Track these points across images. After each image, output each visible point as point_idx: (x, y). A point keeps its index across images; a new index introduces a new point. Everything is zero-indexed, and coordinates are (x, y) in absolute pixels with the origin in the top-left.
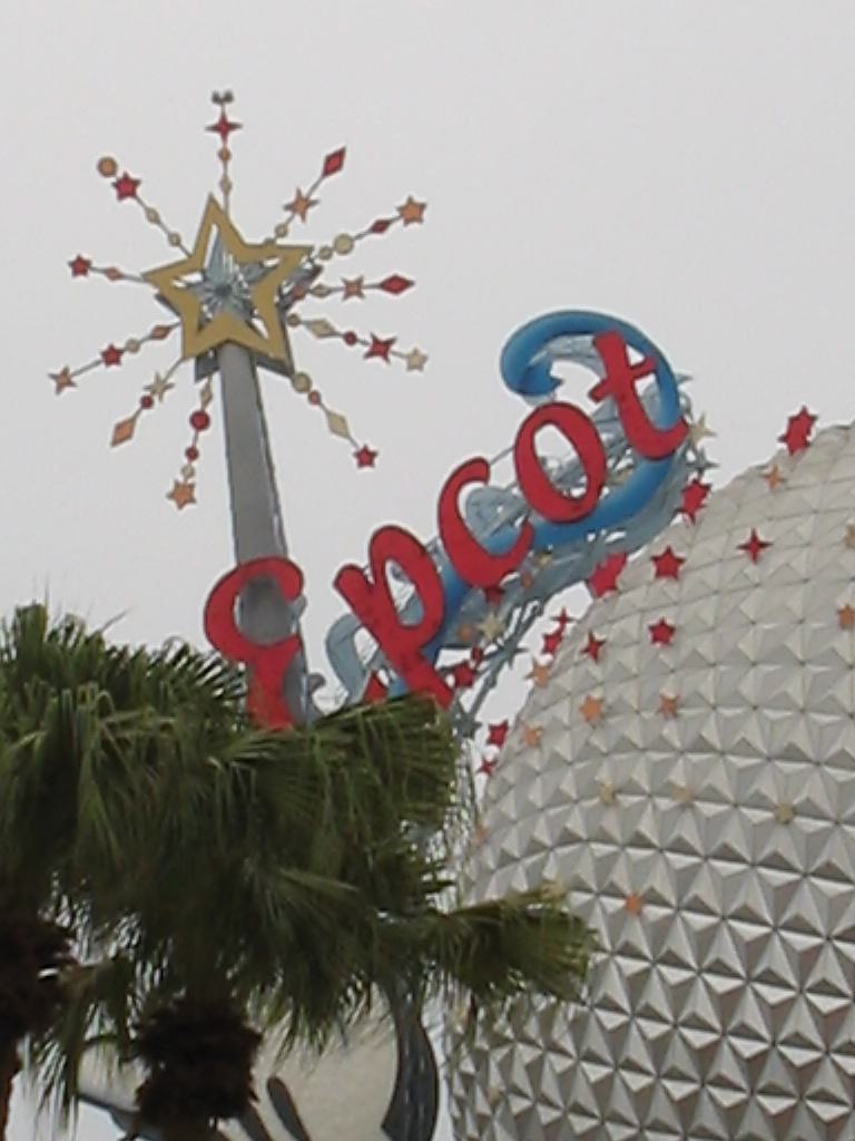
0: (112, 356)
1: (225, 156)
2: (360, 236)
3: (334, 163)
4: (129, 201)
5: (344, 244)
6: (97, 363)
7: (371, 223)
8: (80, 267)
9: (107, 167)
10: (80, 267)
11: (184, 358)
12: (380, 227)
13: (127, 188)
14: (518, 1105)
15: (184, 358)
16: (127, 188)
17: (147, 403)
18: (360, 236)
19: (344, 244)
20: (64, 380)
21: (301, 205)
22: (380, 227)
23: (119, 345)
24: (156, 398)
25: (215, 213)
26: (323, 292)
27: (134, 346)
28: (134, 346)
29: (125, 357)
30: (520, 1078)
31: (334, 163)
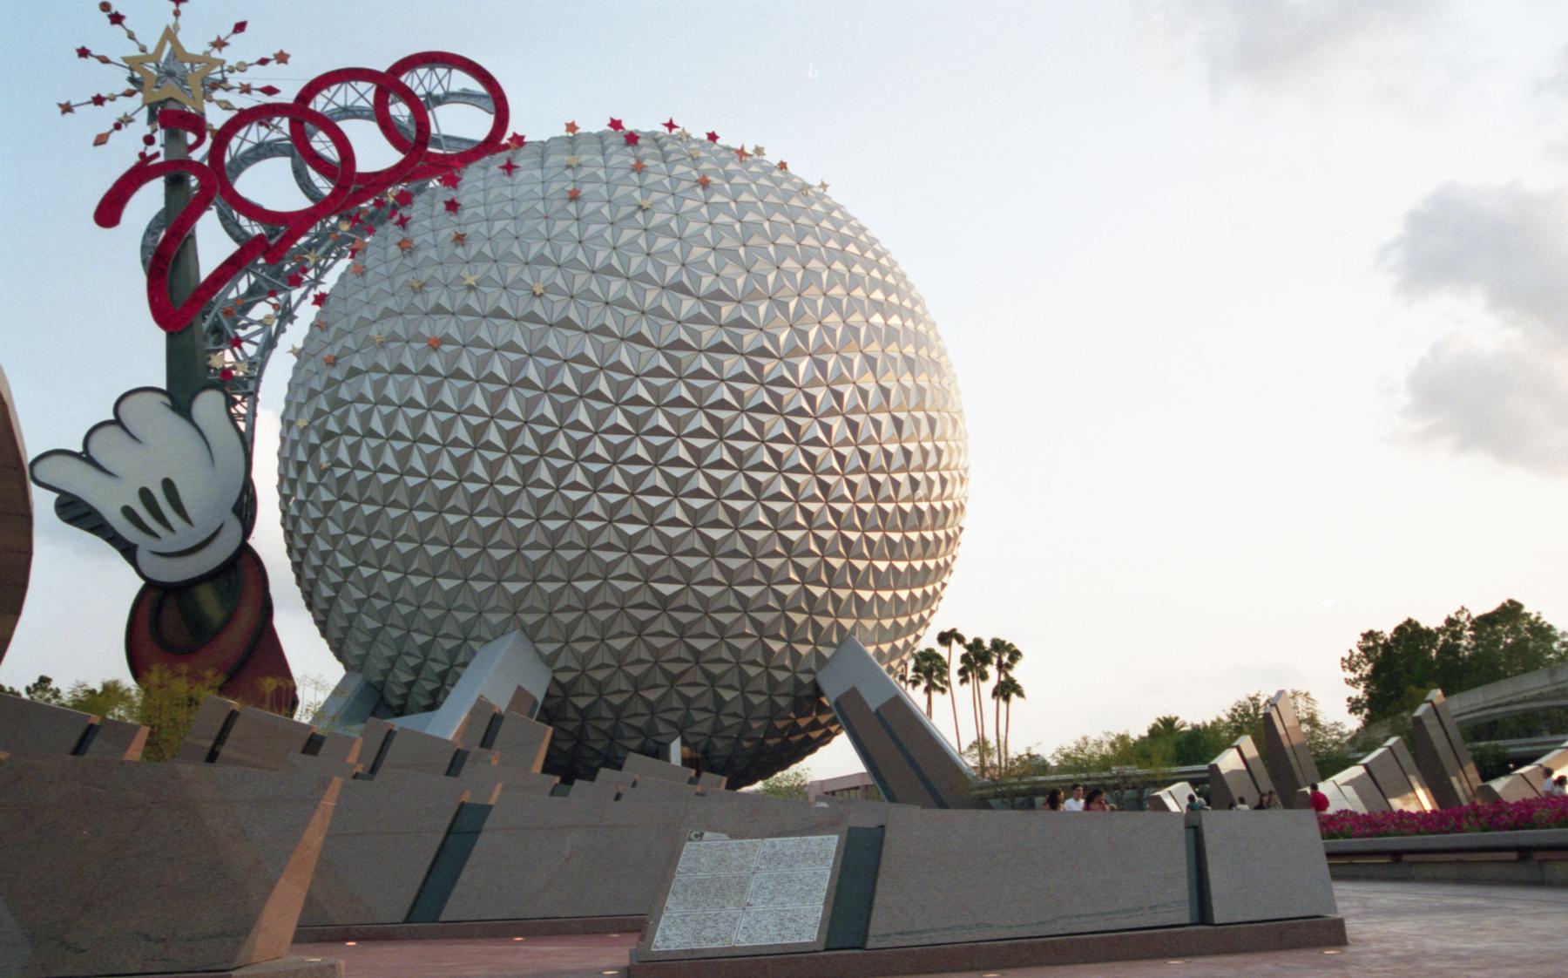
0: (98, 100)
1: (177, 13)
2: (251, 65)
3: (240, 27)
4: (117, 27)
5: (242, 67)
6: (89, 103)
7: (258, 58)
8: (83, 53)
9: (105, 7)
10: (83, 53)
11: (143, 106)
12: (263, 62)
13: (117, 19)
14: (340, 472)
15: (143, 106)
16: (117, 19)
17: (118, 127)
18: (251, 65)
19: (242, 67)
20: (67, 108)
21: (219, 44)
22: (263, 62)
23: (104, 94)
24: (123, 126)
25: (170, 35)
26: (228, 89)
27: (113, 99)
28: (113, 99)
29: (107, 103)
30: (343, 454)
31: (240, 27)
